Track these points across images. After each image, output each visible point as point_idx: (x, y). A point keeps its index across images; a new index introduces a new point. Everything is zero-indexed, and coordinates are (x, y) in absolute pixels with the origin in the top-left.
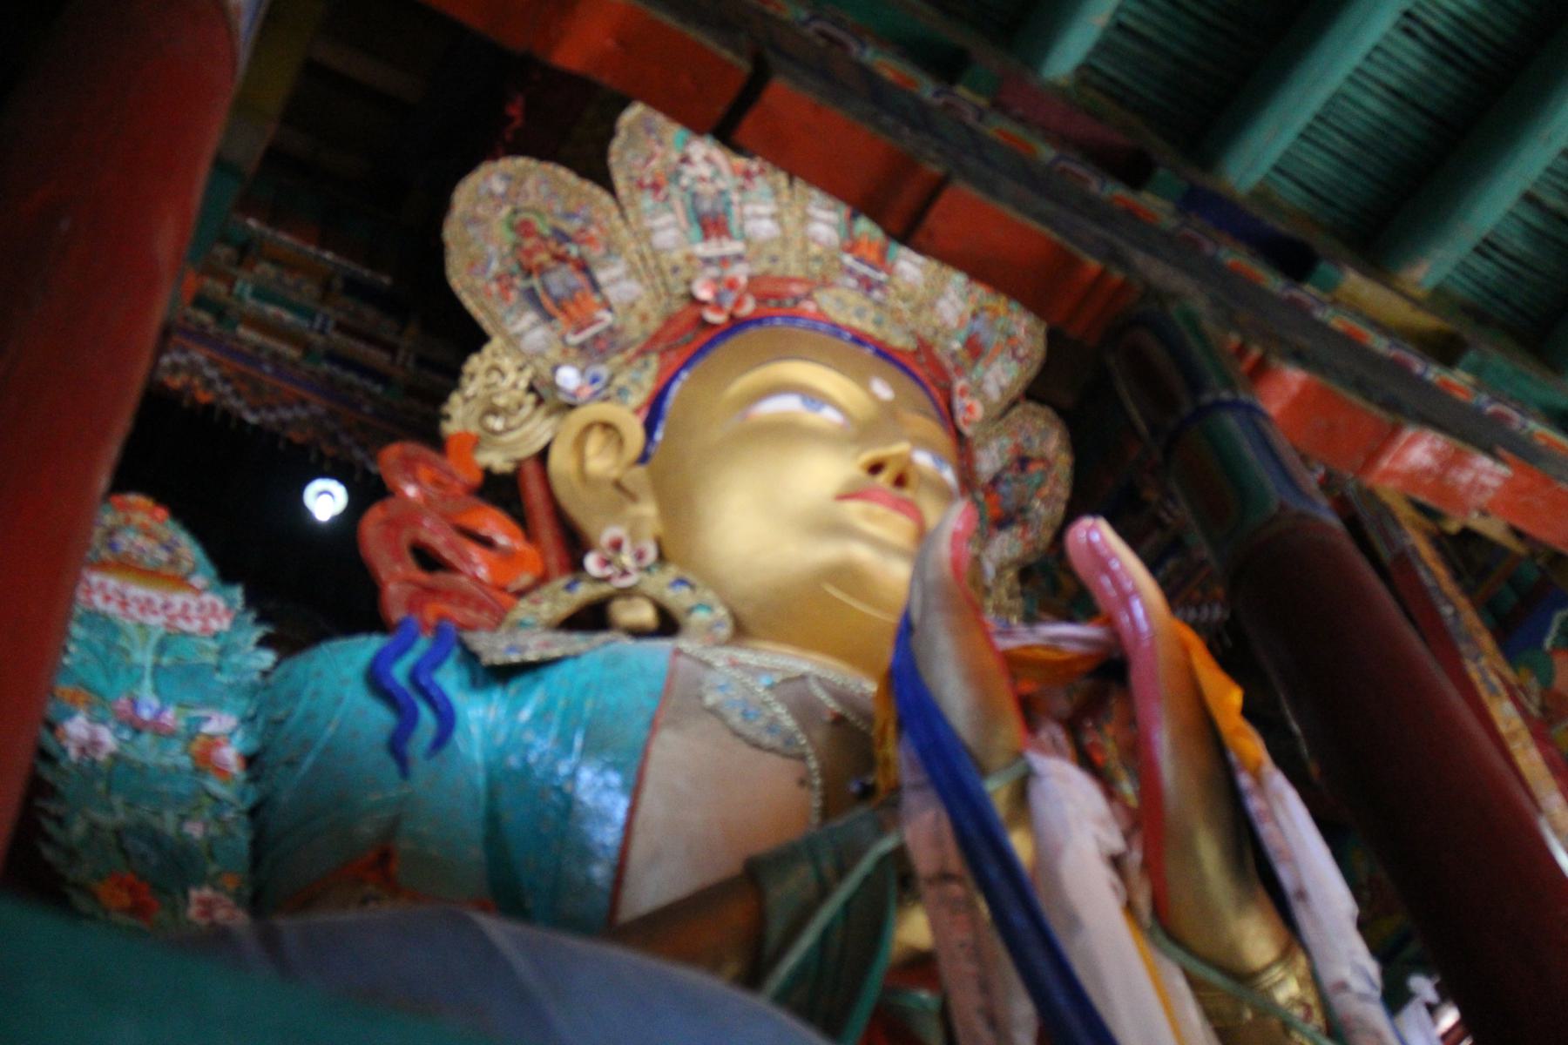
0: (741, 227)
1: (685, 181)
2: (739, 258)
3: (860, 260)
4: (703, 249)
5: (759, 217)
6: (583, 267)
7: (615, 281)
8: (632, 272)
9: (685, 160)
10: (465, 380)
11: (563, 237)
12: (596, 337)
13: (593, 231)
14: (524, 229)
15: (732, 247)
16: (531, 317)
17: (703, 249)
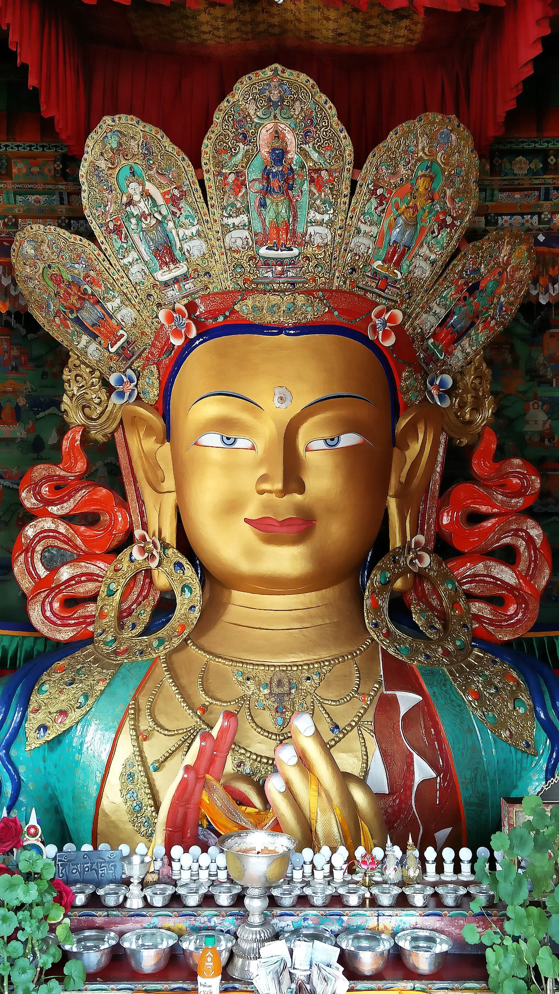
8: (126, 299)
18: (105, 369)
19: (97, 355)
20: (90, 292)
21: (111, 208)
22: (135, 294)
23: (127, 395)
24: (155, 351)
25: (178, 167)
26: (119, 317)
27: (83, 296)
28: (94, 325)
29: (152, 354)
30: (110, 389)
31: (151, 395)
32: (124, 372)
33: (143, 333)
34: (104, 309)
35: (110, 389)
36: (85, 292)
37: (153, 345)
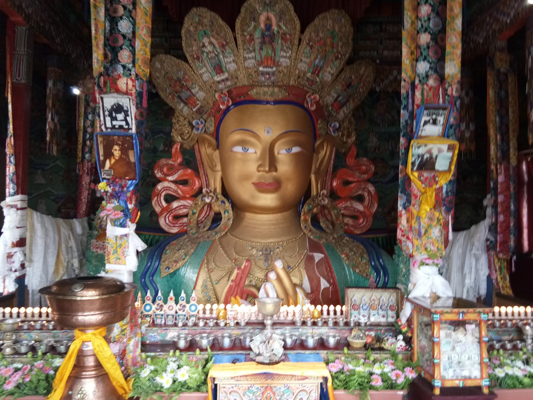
0: (226, 67)
1: (205, 54)
2: (227, 79)
3: (267, 67)
4: (218, 78)
5: (230, 62)
6: (188, 89)
7: (198, 92)
8: (201, 89)
9: (204, 46)
10: (174, 125)
11: (179, 80)
12: (199, 109)
13: (187, 77)
14: (171, 79)
15: (226, 75)
16: (182, 105)
17: (218, 78)
18: (191, 119)
19: (187, 112)
20: (185, 84)
21: (195, 48)
22: (205, 86)
23: (200, 129)
24: (213, 110)
25: (225, 31)
26: (197, 96)
27: (182, 86)
28: (186, 99)
29: (212, 112)
30: (193, 127)
31: (211, 129)
32: (199, 120)
33: (208, 103)
34: (191, 92)
35: (193, 127)
36: (183, 85)
37: (212, 108)
